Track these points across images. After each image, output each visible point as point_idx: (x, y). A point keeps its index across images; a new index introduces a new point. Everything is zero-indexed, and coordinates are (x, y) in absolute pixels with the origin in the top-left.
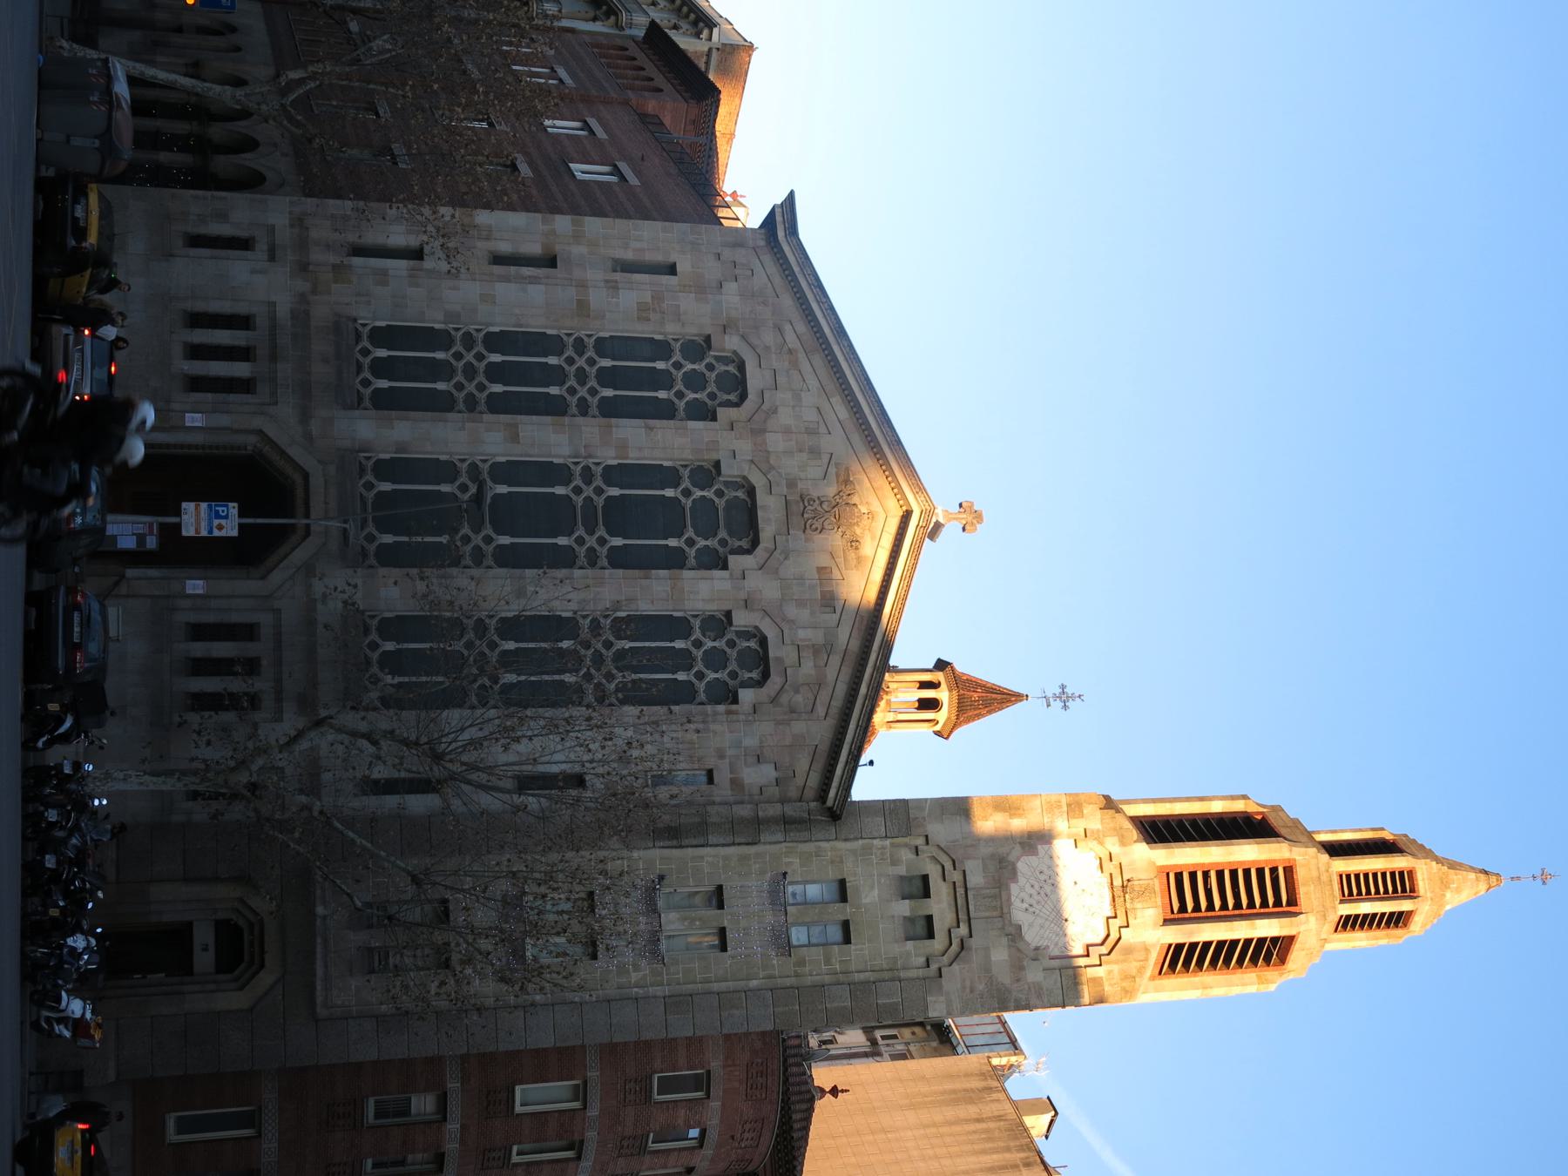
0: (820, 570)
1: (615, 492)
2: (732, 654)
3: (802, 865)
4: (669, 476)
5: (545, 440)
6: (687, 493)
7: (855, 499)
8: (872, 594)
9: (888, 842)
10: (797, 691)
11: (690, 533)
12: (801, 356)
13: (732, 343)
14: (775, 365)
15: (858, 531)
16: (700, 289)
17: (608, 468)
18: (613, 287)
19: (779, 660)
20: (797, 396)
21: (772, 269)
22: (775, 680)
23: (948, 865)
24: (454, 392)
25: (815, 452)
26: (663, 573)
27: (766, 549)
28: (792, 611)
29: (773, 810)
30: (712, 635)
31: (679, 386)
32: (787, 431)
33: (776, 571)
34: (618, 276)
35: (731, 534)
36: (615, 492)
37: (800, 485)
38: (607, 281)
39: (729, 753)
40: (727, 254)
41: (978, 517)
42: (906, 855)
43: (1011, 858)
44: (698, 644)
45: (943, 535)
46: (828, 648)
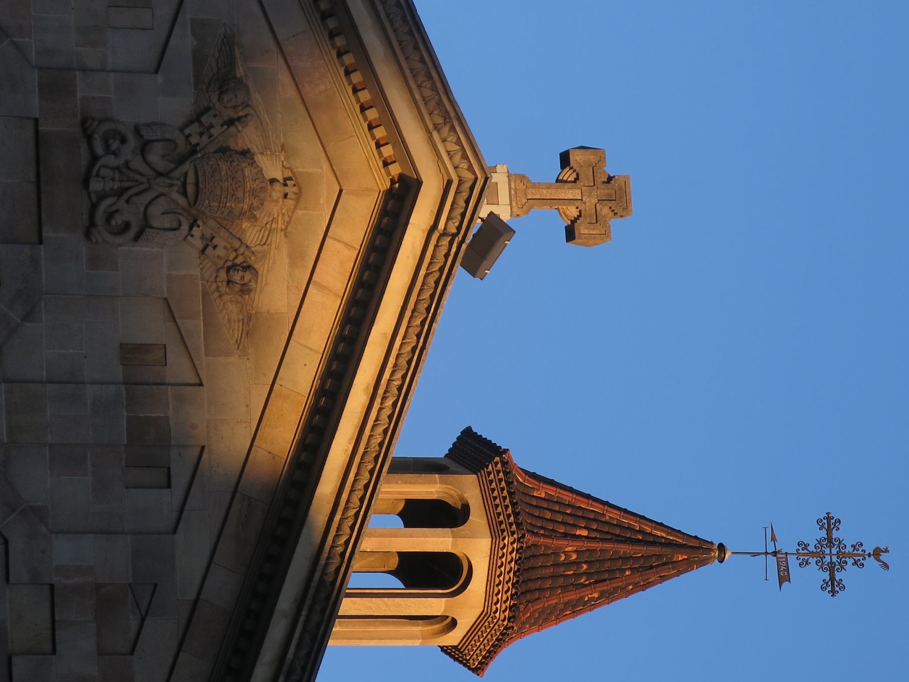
0: (132, 353)
7: (248, 137)
8: (283, 435)
15: (252, 234)
41: (615, 195)
45: (508, 259)
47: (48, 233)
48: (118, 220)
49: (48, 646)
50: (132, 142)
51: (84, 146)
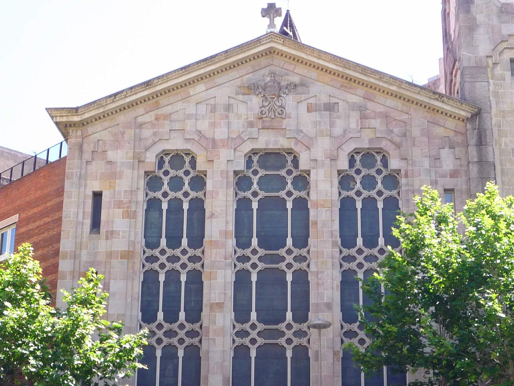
1: (255, 241)
2: (364, 172)
3: (506, 137)
4: (243, 206)
5: (219, 287)
6: (255, 194)
9: (491, 81)
10: (392, 131)
11: (282, 194)
12: (160, 112)
13: (151, 158)
14: (167, 129)
16: (112, 176)
17: (238, 245)
18: (111, 234)
19: (371, 141)
20: (189, 117)
21: (98, 126)
22: (384, 144)
23: (505, 45)
24: (185, 345)
25: (228, 108)
26: (312, 213)
27: (296, 144)
28: (338, 131)
29: (473, 152)
30: (352, 184)
31: (179, 195)
32: (213, 125)
33: (311, 138)
34: (103, 229)
35: (283, 167)
36: (255, 241)
37: (252, 119)
38: (107, 238)
39: (434, 178)
40: (87, 156)
41: (271, 6)
42: (498, 71)
43: (499, 5)
44: (359, 193)
46: (361, 109)
47: (284, 127)
48: (280, 112)
49: (374, 130)
50: (263, 109)
51: (264, 119)
